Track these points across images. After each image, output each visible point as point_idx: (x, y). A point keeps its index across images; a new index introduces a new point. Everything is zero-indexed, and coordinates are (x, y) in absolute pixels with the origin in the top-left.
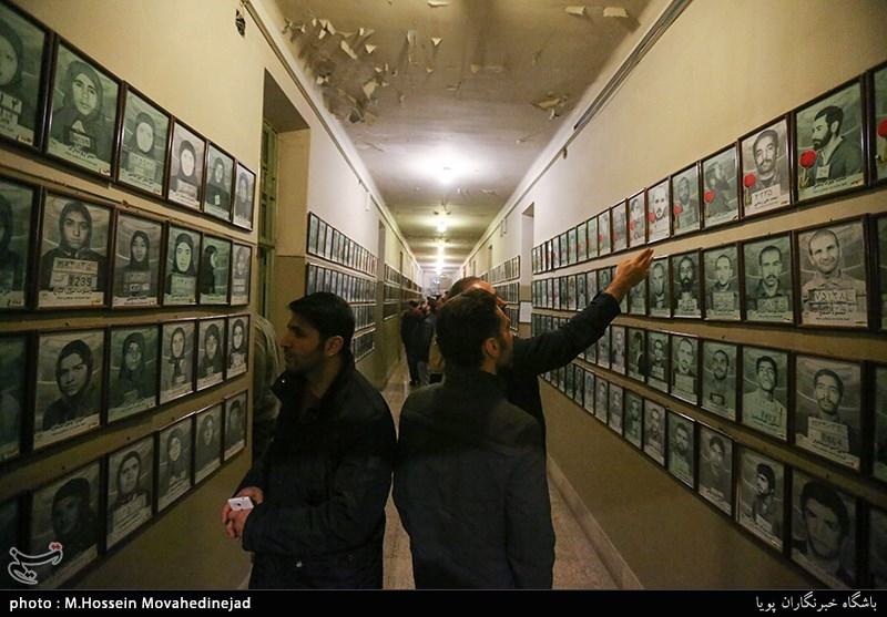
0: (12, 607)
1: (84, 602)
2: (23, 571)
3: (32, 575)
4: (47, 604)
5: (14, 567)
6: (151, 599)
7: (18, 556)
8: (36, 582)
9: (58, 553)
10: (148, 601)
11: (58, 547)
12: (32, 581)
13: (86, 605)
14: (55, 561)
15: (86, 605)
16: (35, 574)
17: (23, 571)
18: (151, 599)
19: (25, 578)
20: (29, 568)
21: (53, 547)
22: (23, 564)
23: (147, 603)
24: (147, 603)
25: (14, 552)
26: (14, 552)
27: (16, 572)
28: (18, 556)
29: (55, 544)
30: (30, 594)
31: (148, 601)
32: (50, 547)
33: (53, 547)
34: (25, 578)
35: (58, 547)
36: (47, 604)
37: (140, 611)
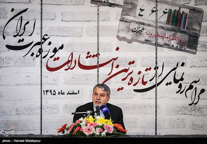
0: (3, 142)
1: (14, 141)
2: (5, 133)
4: (10, 141)
6: (28, 140)
7: (4, 130)
8: (8, 136)
9: (13, 129)
10: (27, 140)
11: (13, 128)
13: (15, 141)
15: (15, 141)
17: (5, 133)
18: (28, 140)
20: (7, 133)
21: (12, 128)
22: (5, 132)
23: (27, 141)
24: (27, 141)
25: (3, 129)
26: (3, 129)
27: (4, 134)
28: (4, 130)
29: (13, 127)
30: (6, 139)
31: (27, 140)
32: (11, 128)
33: (12, 128)
36: (10, 141)
37: (25, 142)
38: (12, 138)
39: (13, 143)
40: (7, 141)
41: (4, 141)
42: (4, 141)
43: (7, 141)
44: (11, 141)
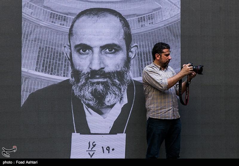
0: (3, 163)
3: (8, 155)
4: (11, 162)
5: (3, 153)
7: (5, 150)
8: (9, 157)
9: (15, 149)
11: (15, 147)
12: (8, 156)
14: (14, 151)
16: (9, 155)
17: (6, 154)
19: (7, 155)
22: (5, 152)
25: (3, 148)
26: (3, 148)
27: (4, 154)
28: (5, 150)
30: (7, 160)
32: (13, 147)
34: (7, 155)
35: (15, 147)
36: (11, 162)
38: (14, 160)
39: (15, 164)
40: (8, 162)
41: (4, 163)
42: (4, 163)
43: (8, 162)
44: (13, 163)
